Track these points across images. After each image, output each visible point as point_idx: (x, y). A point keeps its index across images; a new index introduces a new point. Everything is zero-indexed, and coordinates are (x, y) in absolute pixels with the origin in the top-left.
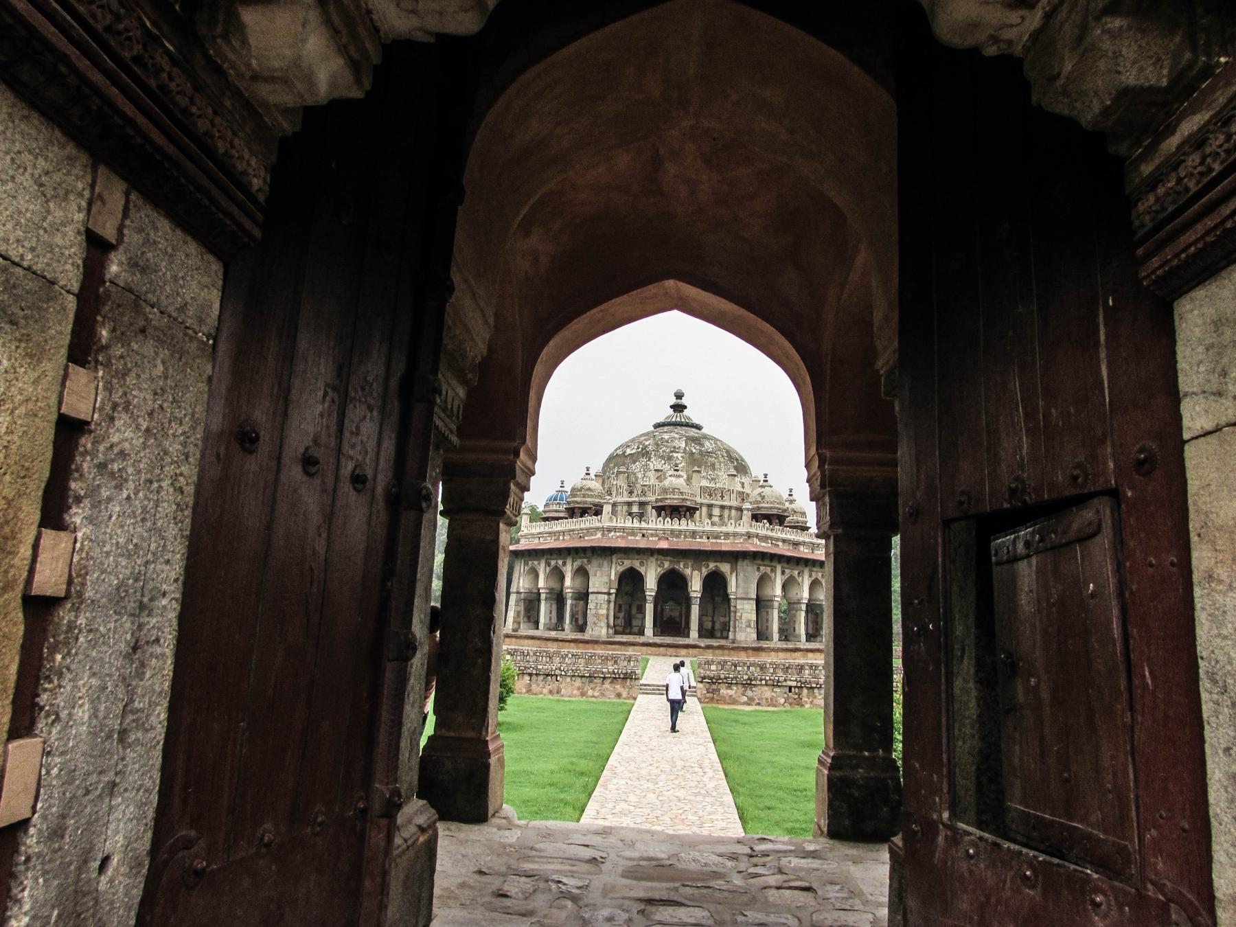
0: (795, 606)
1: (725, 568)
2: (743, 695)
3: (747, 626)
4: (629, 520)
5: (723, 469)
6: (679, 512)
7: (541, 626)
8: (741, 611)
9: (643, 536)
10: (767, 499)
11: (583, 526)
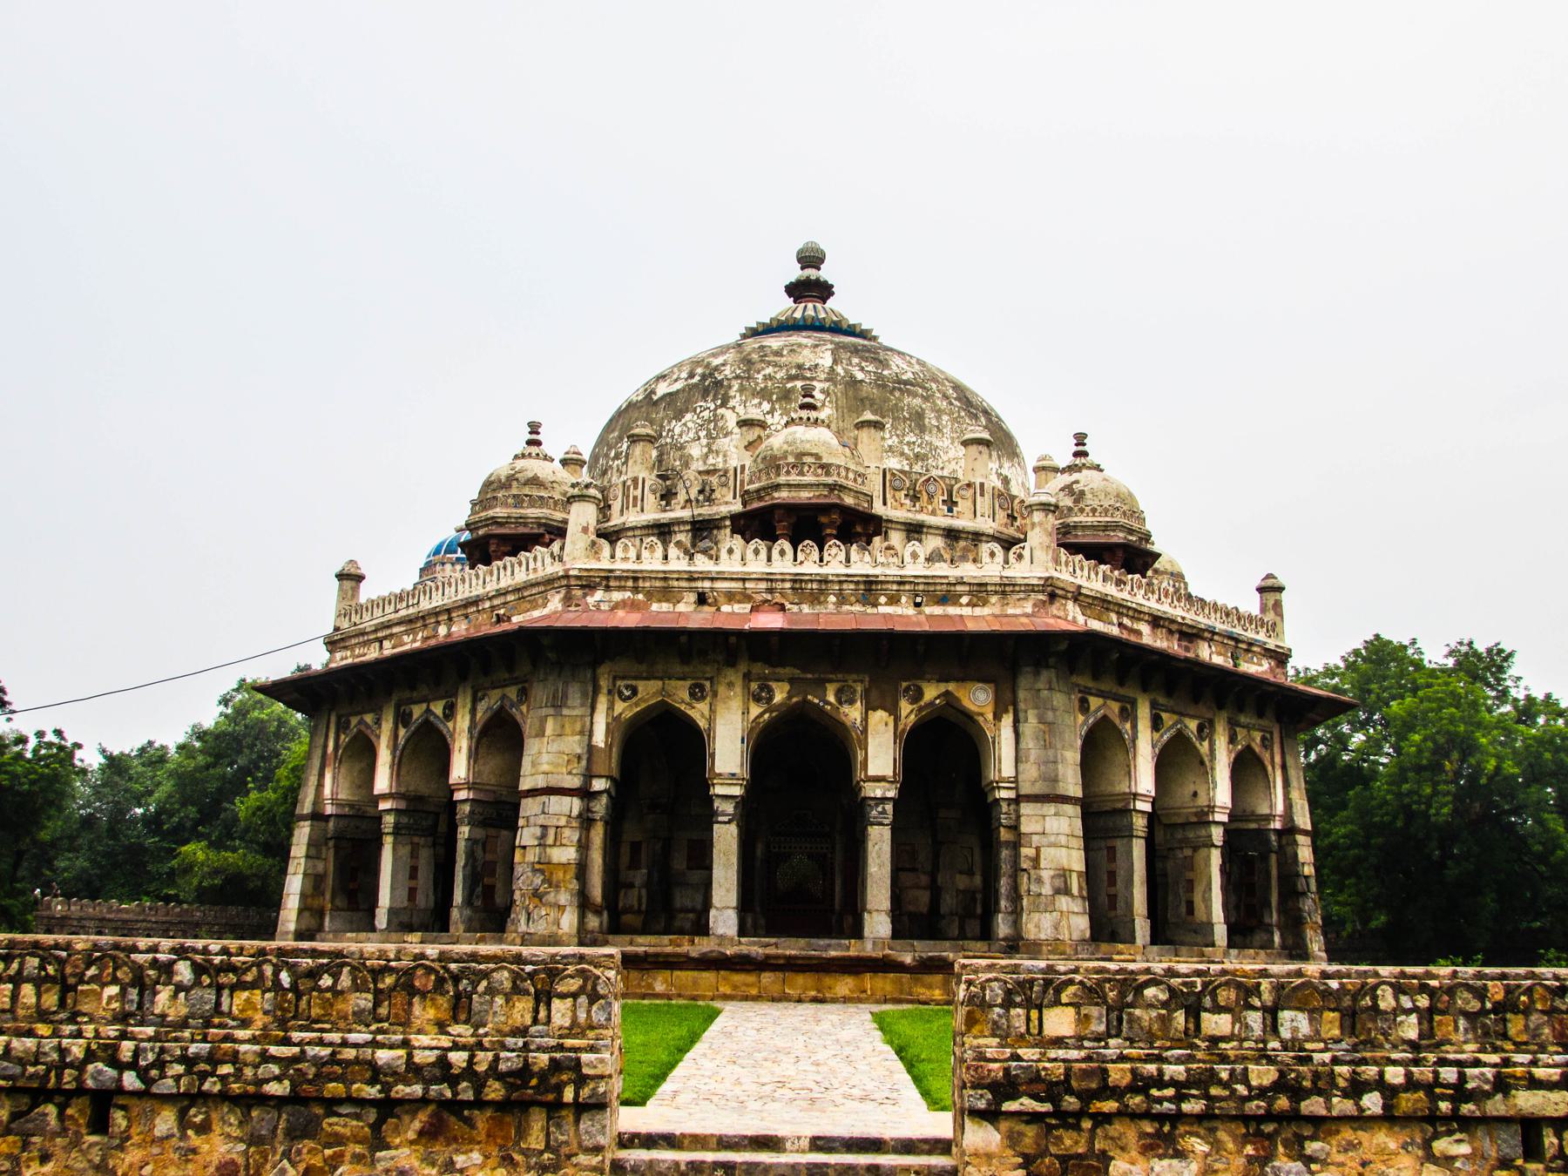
1: (977, 699)
3: (1057, 892)
4: (652, 548)
6: (821, 527)
7: (381, 920)
8: (1035, 838)
9: (702, 599)
10: (1090, 500)
11: (506, 582)
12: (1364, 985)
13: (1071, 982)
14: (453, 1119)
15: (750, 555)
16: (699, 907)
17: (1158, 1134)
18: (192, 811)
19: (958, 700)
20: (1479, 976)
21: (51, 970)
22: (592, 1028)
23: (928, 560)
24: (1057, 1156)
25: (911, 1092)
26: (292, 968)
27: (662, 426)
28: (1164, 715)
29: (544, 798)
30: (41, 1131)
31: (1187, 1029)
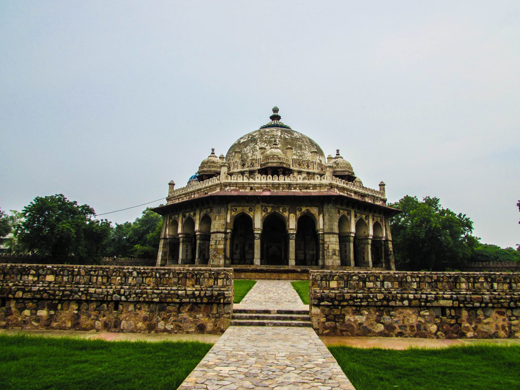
0: (364, 241)
1: (314, 211)
2: (378, 321)
4: (240, 177)
5: (307, 149)
7: (180, 262)
9: (251, 189)
12: (404, 276)
13: (336, 275)
14: (196, 308)
15: (262, 178)
16: (251, 258)
17: (356, 310)
18: (137, 237)
19: (310, 211)
20: (431, 274)
21: (105, 273)
22: (227, 286)
23: (303, 179)
24: (333, 315)
25: (300, 300)
26: (159, 273)
27: (242, 150)
28: (357, 214)
29: (216, 234)
30: (103, 310)
31: (363, 286)
